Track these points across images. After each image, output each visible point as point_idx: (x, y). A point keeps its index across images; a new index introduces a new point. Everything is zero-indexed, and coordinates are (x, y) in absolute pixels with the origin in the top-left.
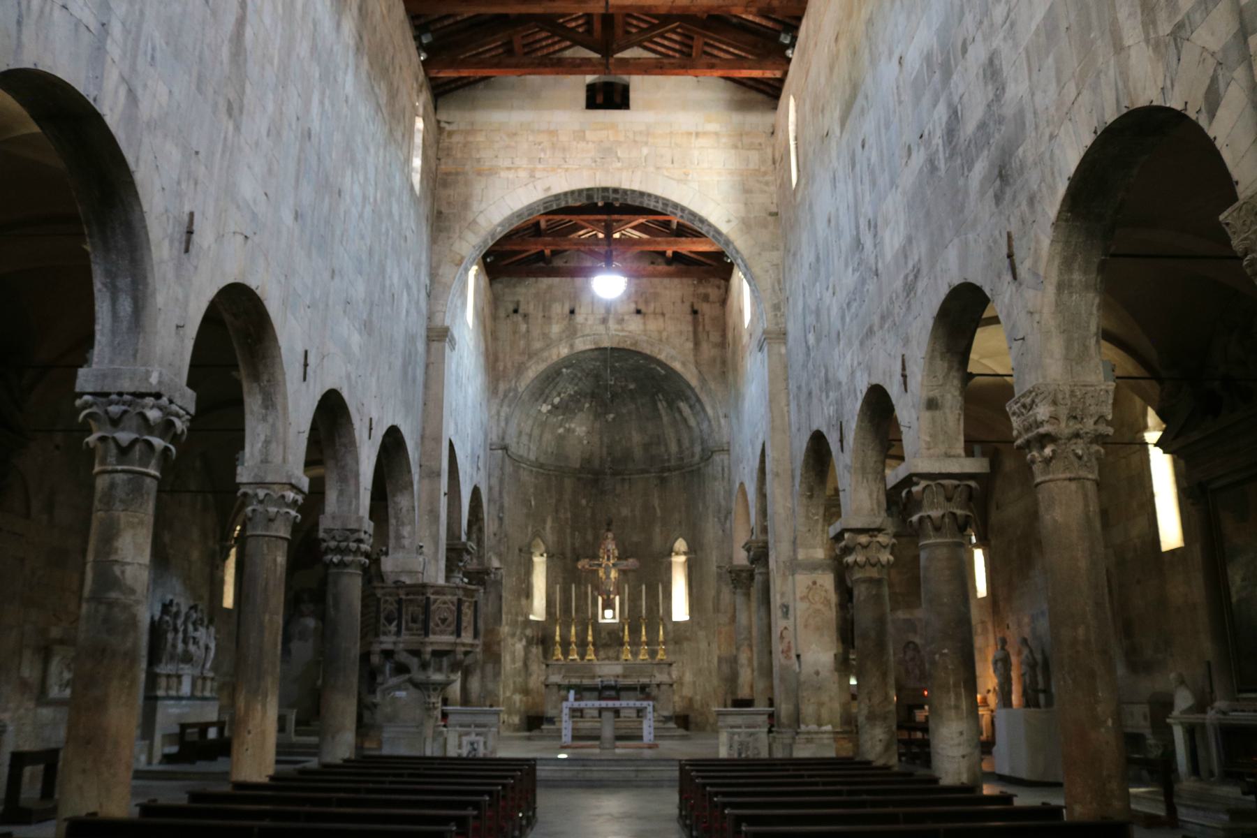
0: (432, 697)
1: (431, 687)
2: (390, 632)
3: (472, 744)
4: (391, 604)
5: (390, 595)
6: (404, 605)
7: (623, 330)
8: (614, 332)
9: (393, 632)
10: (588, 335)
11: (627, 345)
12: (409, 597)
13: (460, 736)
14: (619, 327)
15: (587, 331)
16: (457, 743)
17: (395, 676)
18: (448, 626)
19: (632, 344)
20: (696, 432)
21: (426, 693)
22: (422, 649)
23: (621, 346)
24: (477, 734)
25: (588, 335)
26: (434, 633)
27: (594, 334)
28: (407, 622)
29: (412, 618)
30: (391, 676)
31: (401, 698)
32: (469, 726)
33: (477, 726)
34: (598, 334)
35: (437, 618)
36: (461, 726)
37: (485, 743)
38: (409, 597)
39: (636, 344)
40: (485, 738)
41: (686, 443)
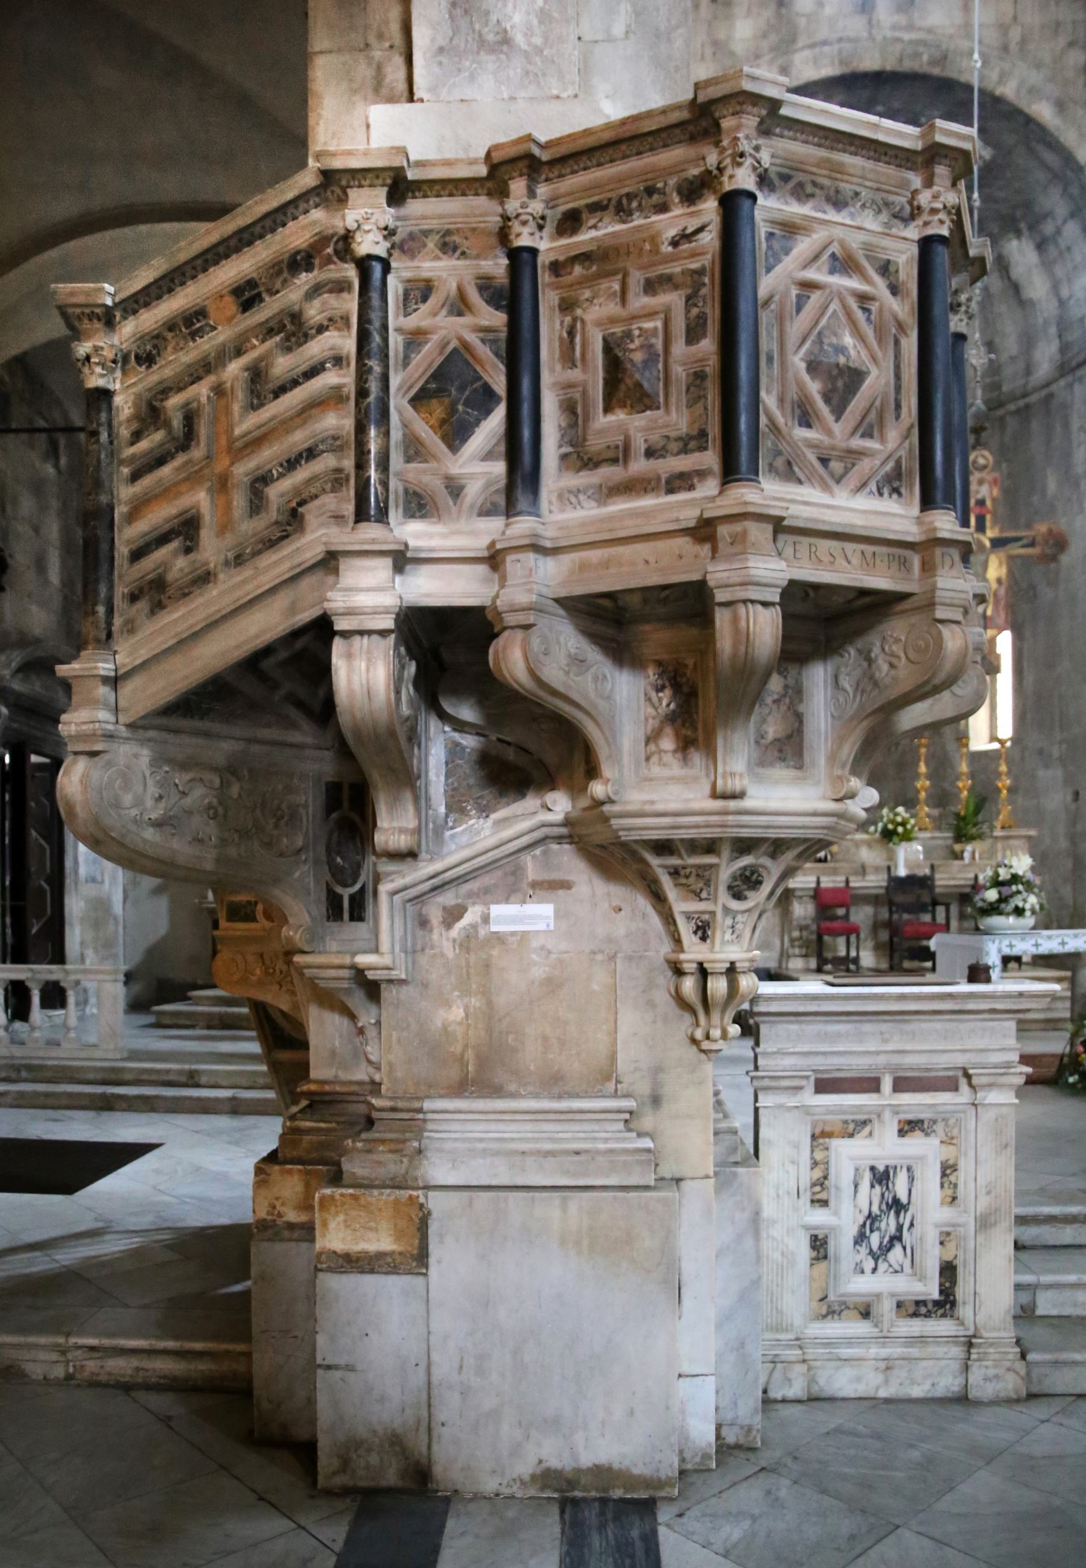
0: (721, 933)
1: (727, 868)
2: (455, 489)
3: (882, 1177)
4: (460, 306)
5: (447, 247)
6: (549, 299)
7: (911, 27)
8: (889, 34)
9: (473, 491)
10: (825, 43)
11: (922, 64)
12: (586, 237)
13: (820, 1136)
14: (902, 20)
15: (823, 33)
16: (807, 1176)
17: (485, 811)
18: (868, 429)
19: (933, 62)
20: (1047, 308)
21: (681, 905)
22: (718, 573)
23: (908, 66)
24: (909, 1127)
25: (825, 43)
26: (789, 473)
27: (840, 40)
28: (569, 408)
29: (614, 366)
30: (456, 807)
31: (524, 936)
32: (871, 1085)
33: (901, 1085)
34: (850, 40)
35: (798, 362)
36: (824, 1086)
37: (947, 1170)
38: (586, 237)
39: (943, 59)
40: (949, 1141)
41: (1010, 345)
